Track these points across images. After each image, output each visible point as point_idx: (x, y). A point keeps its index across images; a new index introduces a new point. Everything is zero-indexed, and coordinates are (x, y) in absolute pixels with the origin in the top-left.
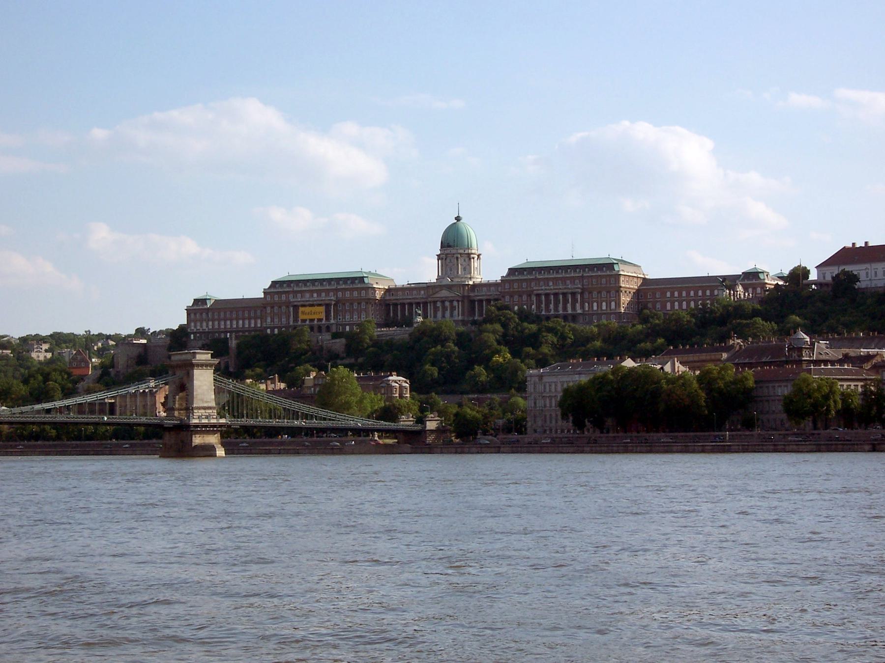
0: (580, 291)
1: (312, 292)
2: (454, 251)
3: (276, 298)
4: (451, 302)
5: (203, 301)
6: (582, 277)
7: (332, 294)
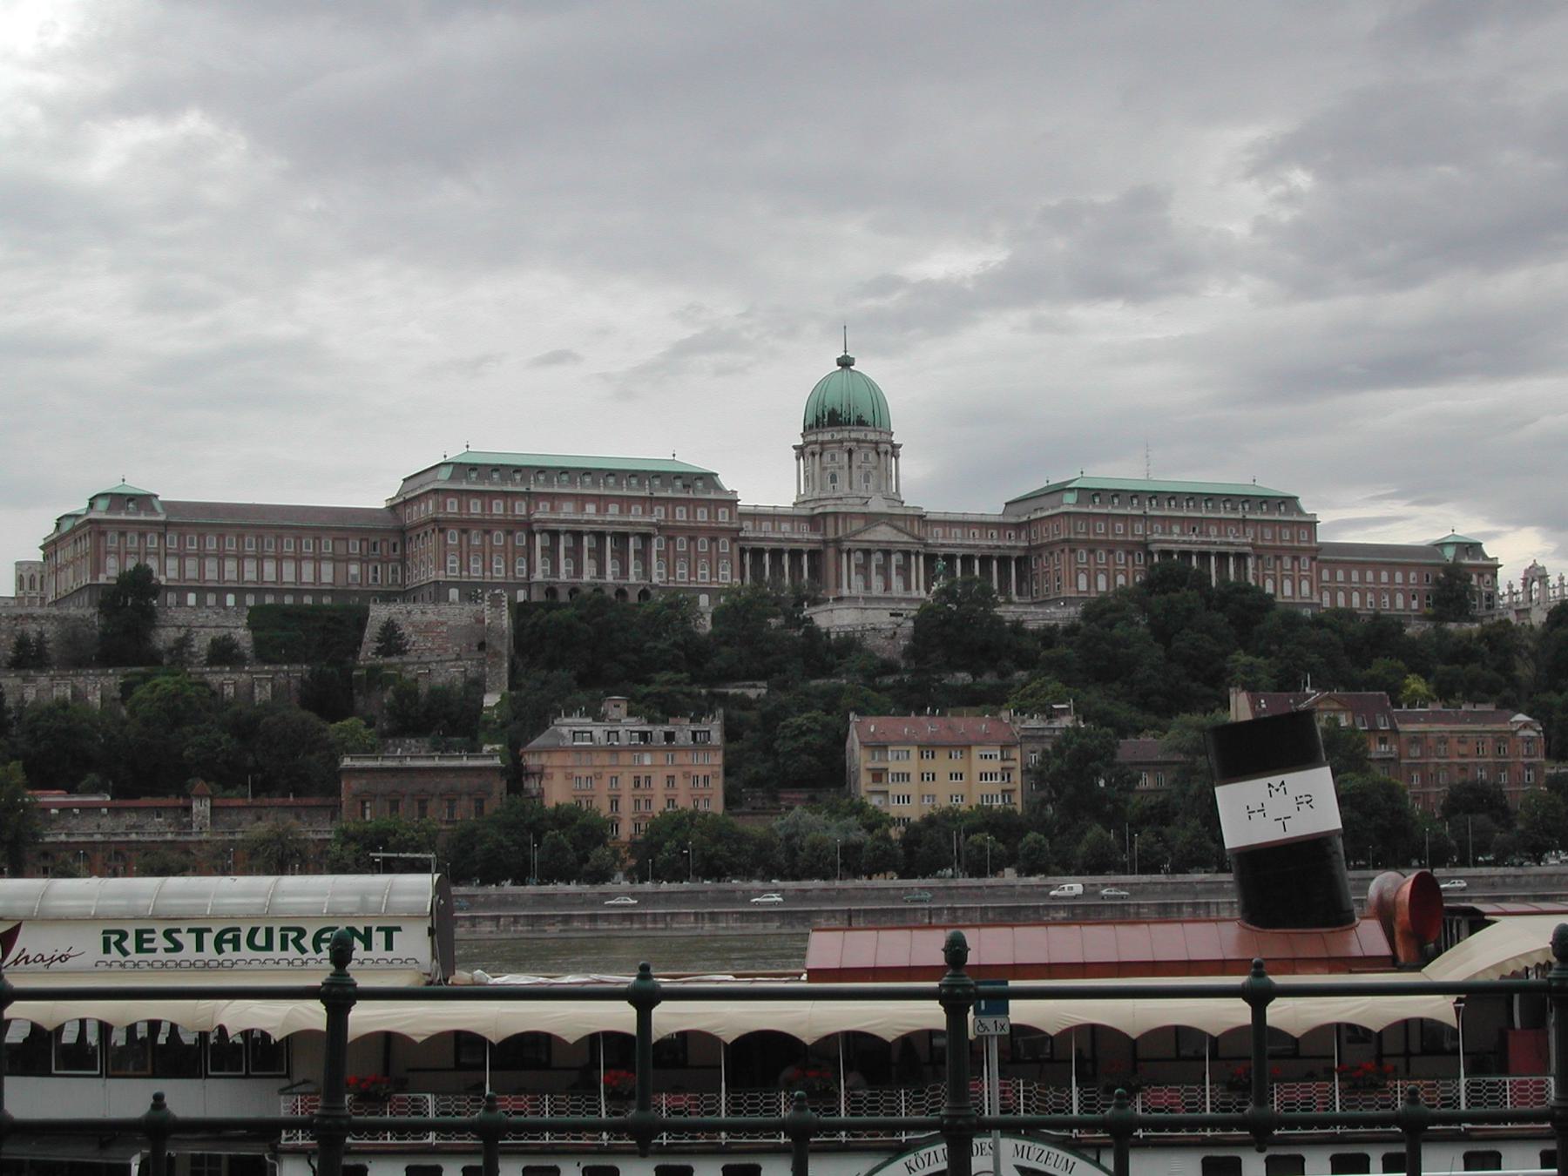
0: (1248, 549)
1: (581, 499)
2: (872, 436)
3: (475, 508)
4: (907, 554)
5: (144, 500)
6: (1244, 521)
7: (636, 509)
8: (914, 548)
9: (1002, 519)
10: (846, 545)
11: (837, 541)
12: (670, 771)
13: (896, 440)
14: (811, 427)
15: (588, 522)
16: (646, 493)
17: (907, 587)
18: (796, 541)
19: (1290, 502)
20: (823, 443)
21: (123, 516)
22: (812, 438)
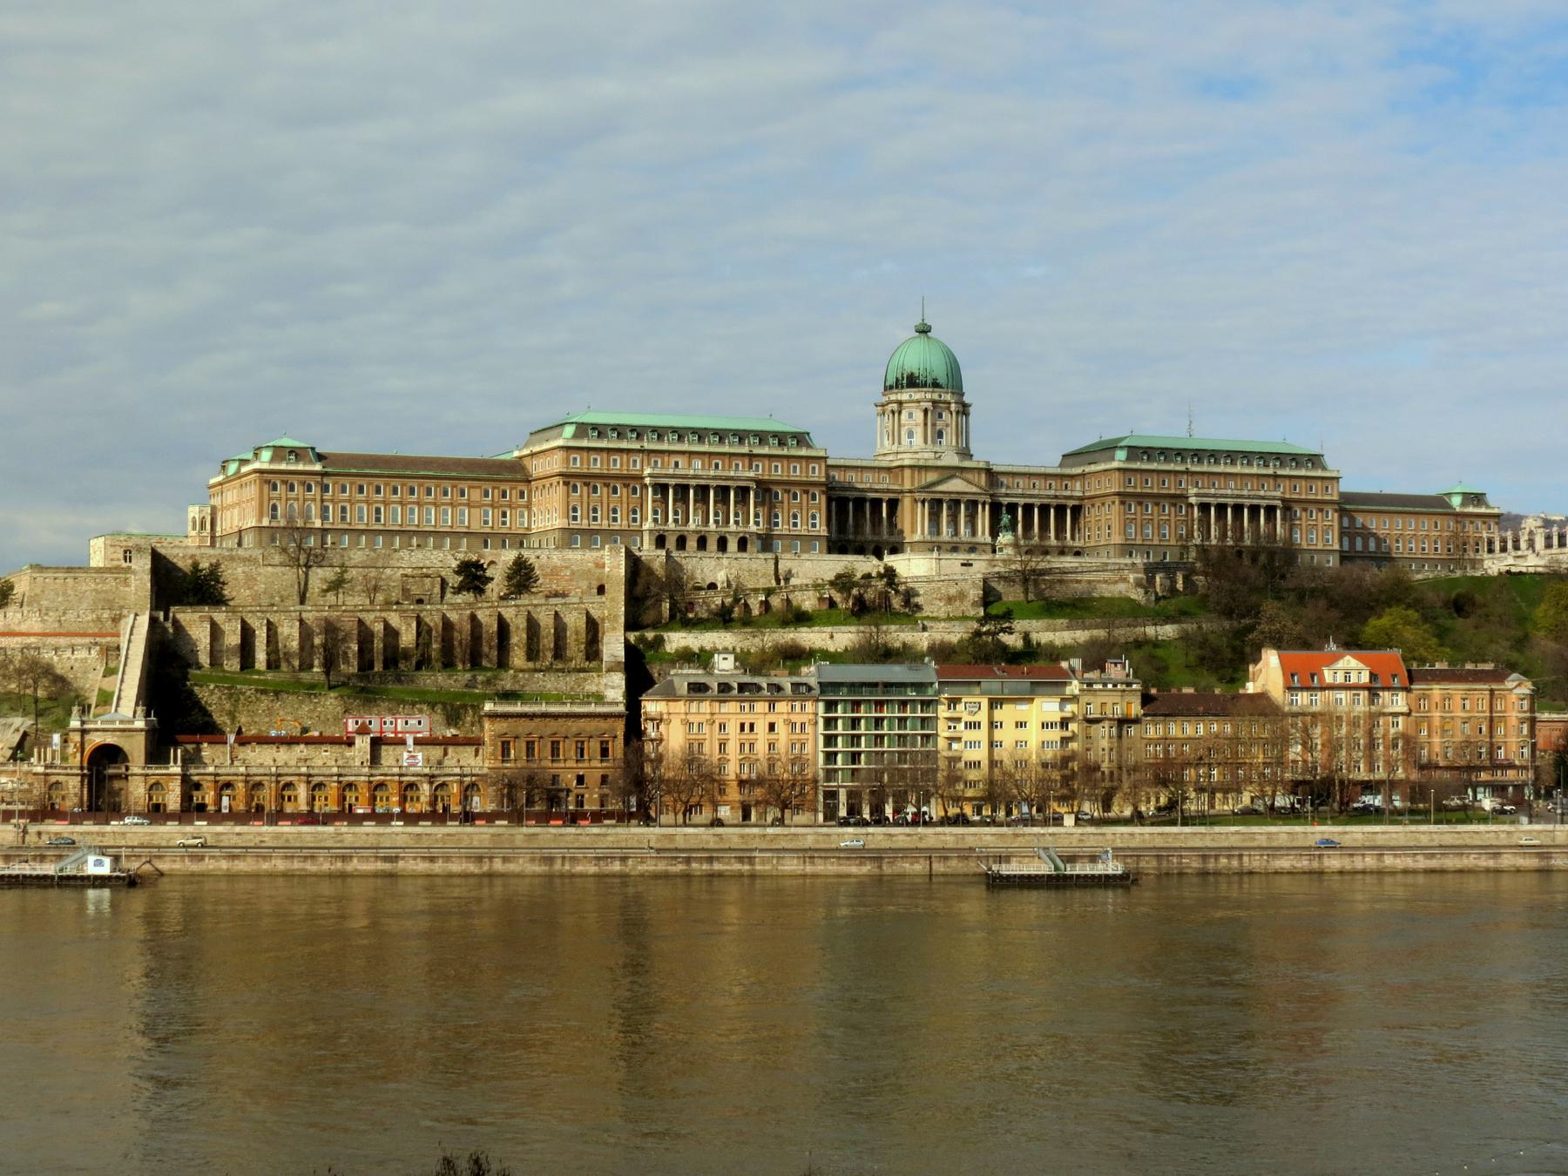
0: (1279, 503)
6: (1276, 476)
8: (981, 499)
9: (1059, 471)
10: (923, 496)
11: (910, 491)
12: (771, 718)
13: (966, 399)
14: (891, 387)
15: (695, 477)
16: (745, 450)
17: (974, 533)
18: (876, 491)
19: (1315, 460)
20: (900, 403)
21: (283, 466)
22: (893, 397)
